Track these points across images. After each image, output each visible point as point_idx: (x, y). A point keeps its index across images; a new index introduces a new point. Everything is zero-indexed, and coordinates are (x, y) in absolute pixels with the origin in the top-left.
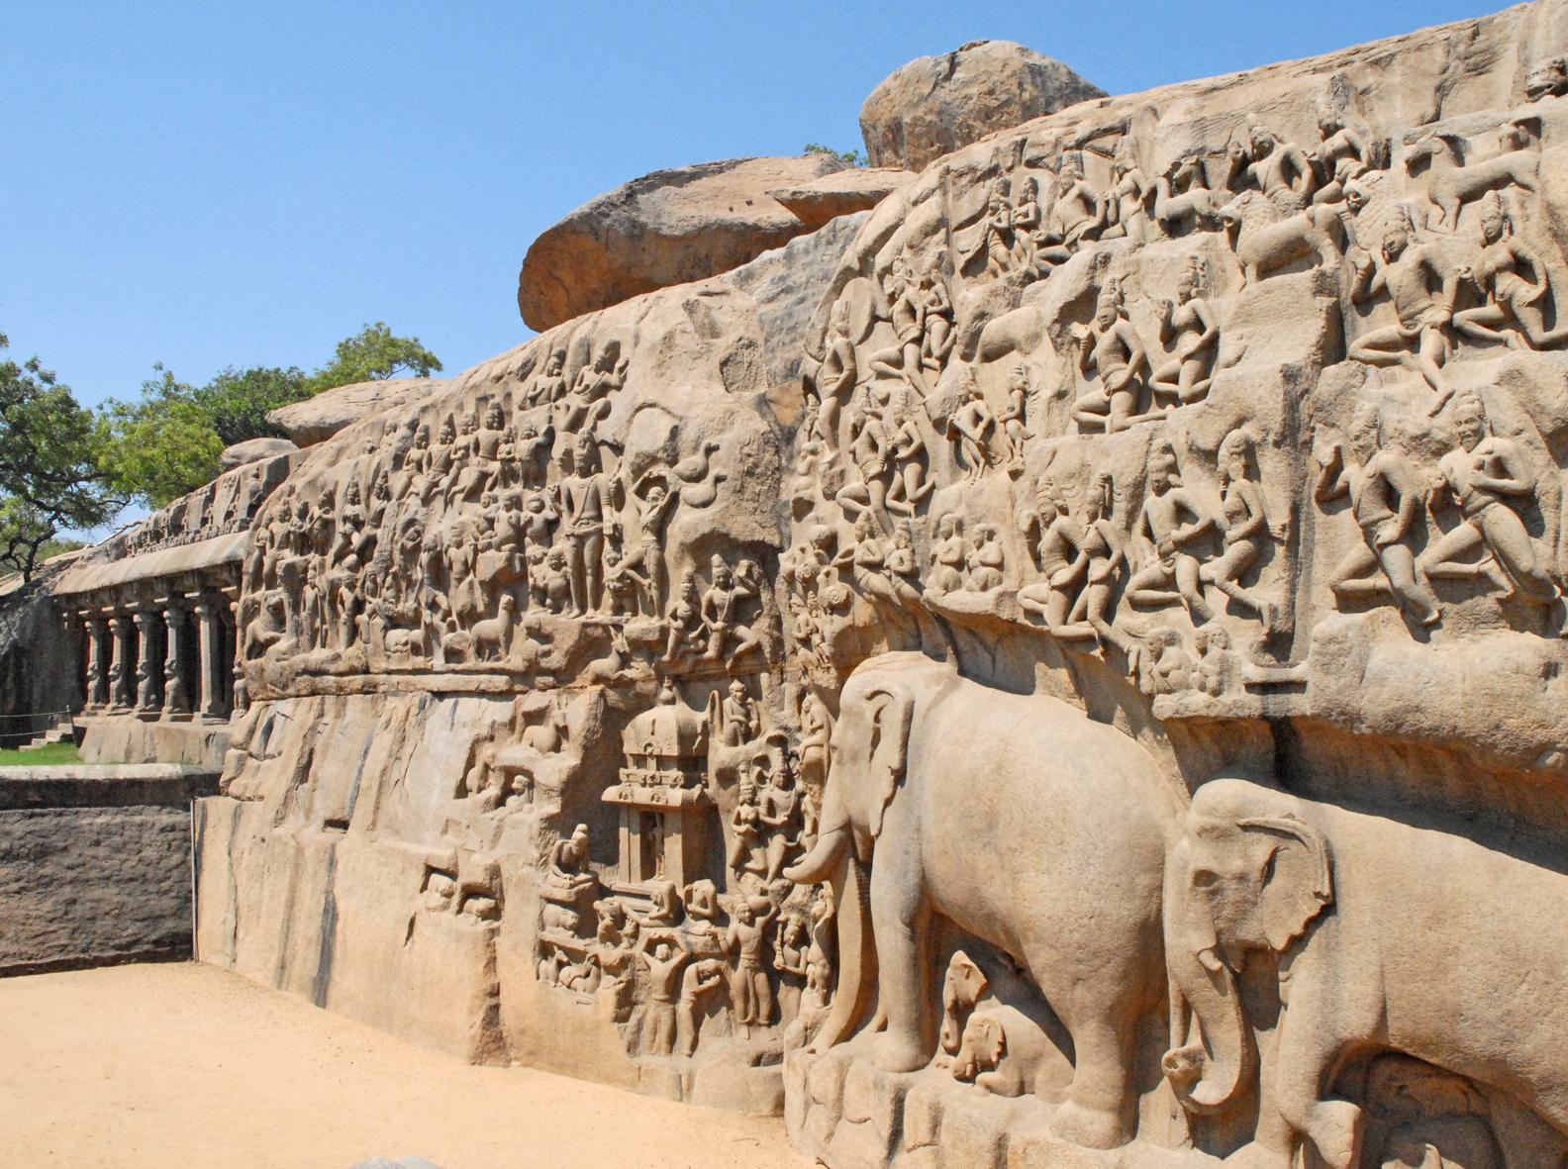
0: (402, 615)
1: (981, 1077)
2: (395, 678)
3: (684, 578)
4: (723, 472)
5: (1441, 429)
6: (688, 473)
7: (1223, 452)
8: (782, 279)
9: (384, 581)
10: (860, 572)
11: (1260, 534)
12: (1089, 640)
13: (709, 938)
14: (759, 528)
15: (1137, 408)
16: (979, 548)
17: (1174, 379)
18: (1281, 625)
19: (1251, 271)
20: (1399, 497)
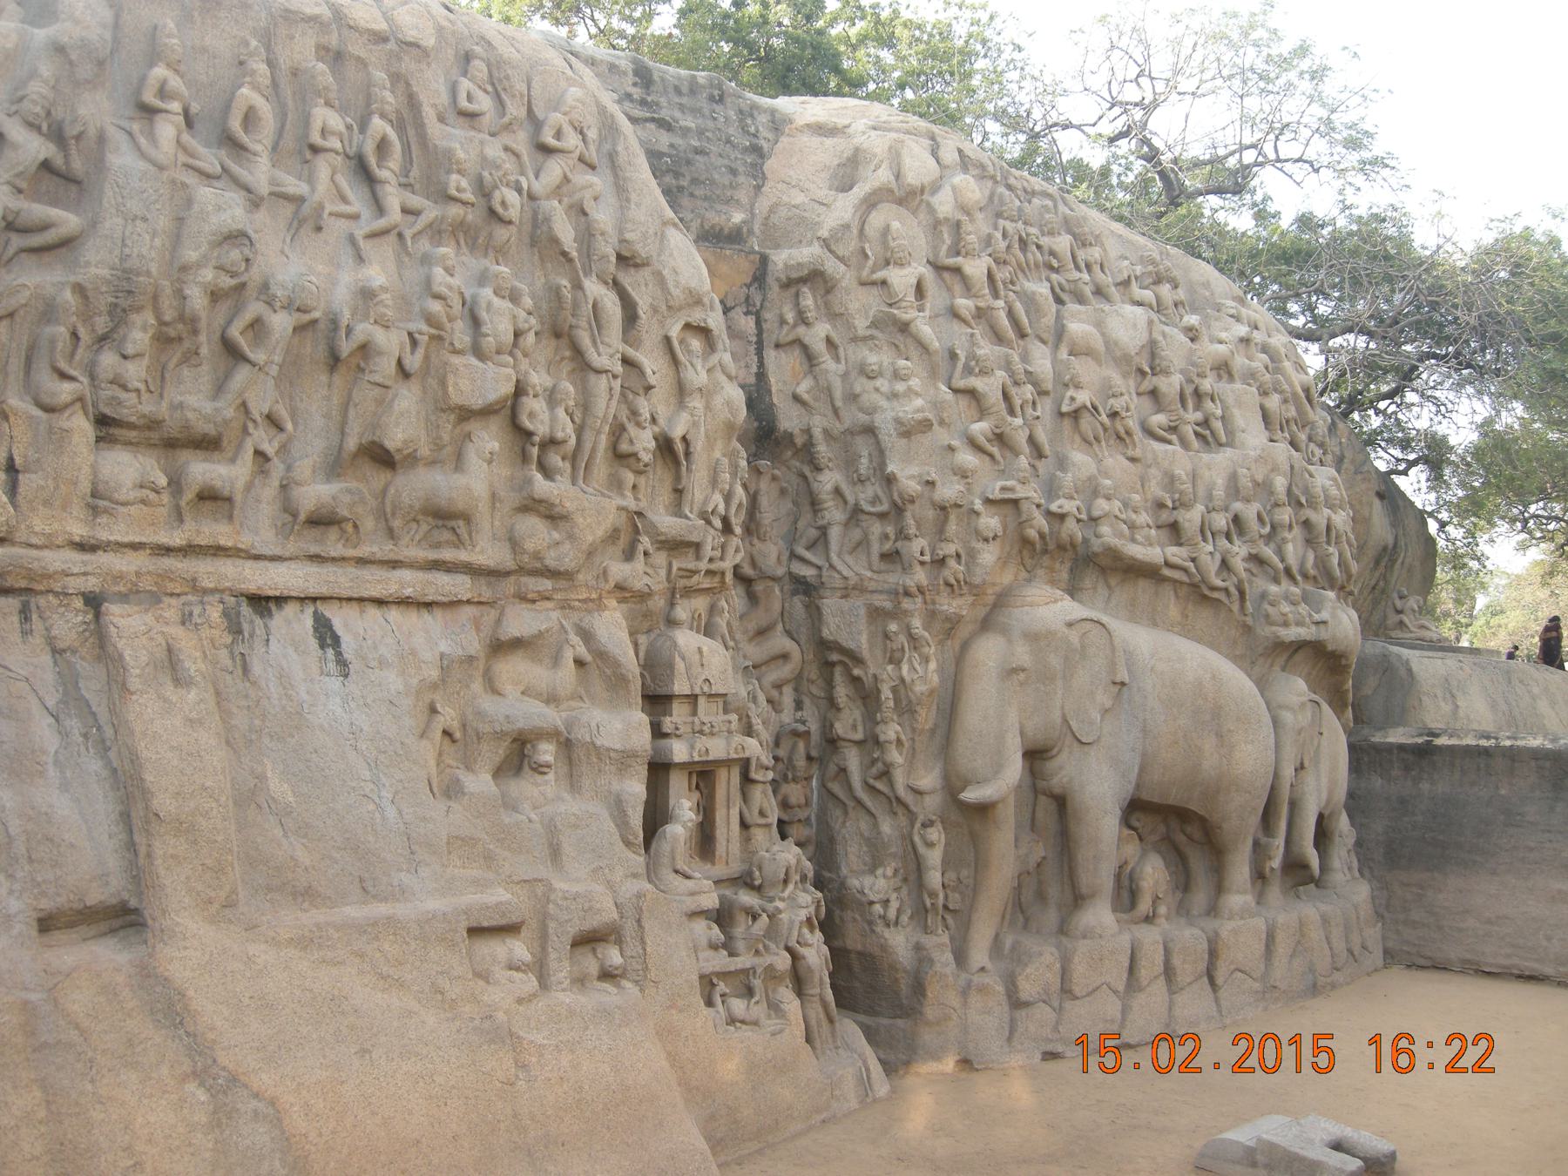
0: (153, 424)
2: (126, 563)
9: (103, 339)
12: (1226, 590)
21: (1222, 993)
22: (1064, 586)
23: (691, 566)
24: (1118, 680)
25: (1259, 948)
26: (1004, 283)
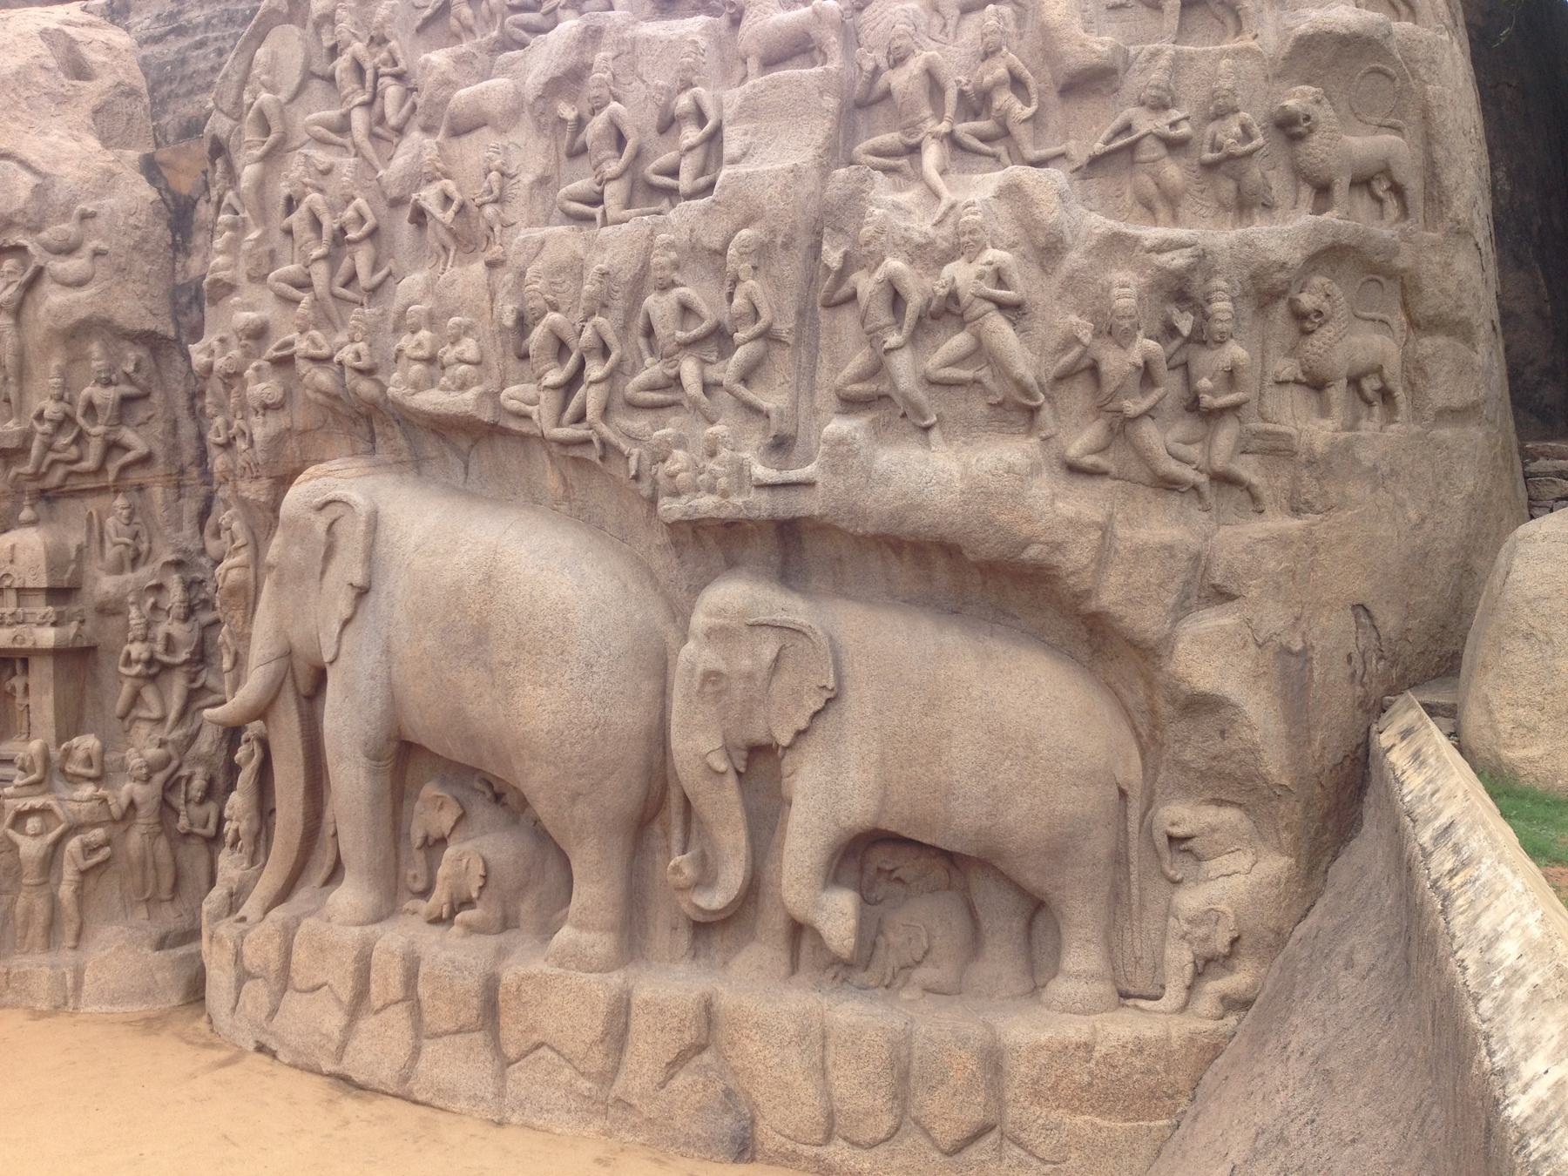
1: (458, 917)
3: (53, 372)
4: (104, 246)
5: (945, 239)
6: (56, 243)
7: (731, 251)
8: (172, 16)
10: (303, 367)
11: (767, 336)
12: (587, 442)
13: (95, 803)
14: (150, 317)
15: (629, 204)
16: (453, 344)
17: (674, 173)
18: (788, 429)
19: (753, 64)
20: (905, 304)
21: (514, 1073)
22: (405, 456)
23: (22, 470)
24: (349, 579)
25: (593, 1025)
26: (376, 69)
